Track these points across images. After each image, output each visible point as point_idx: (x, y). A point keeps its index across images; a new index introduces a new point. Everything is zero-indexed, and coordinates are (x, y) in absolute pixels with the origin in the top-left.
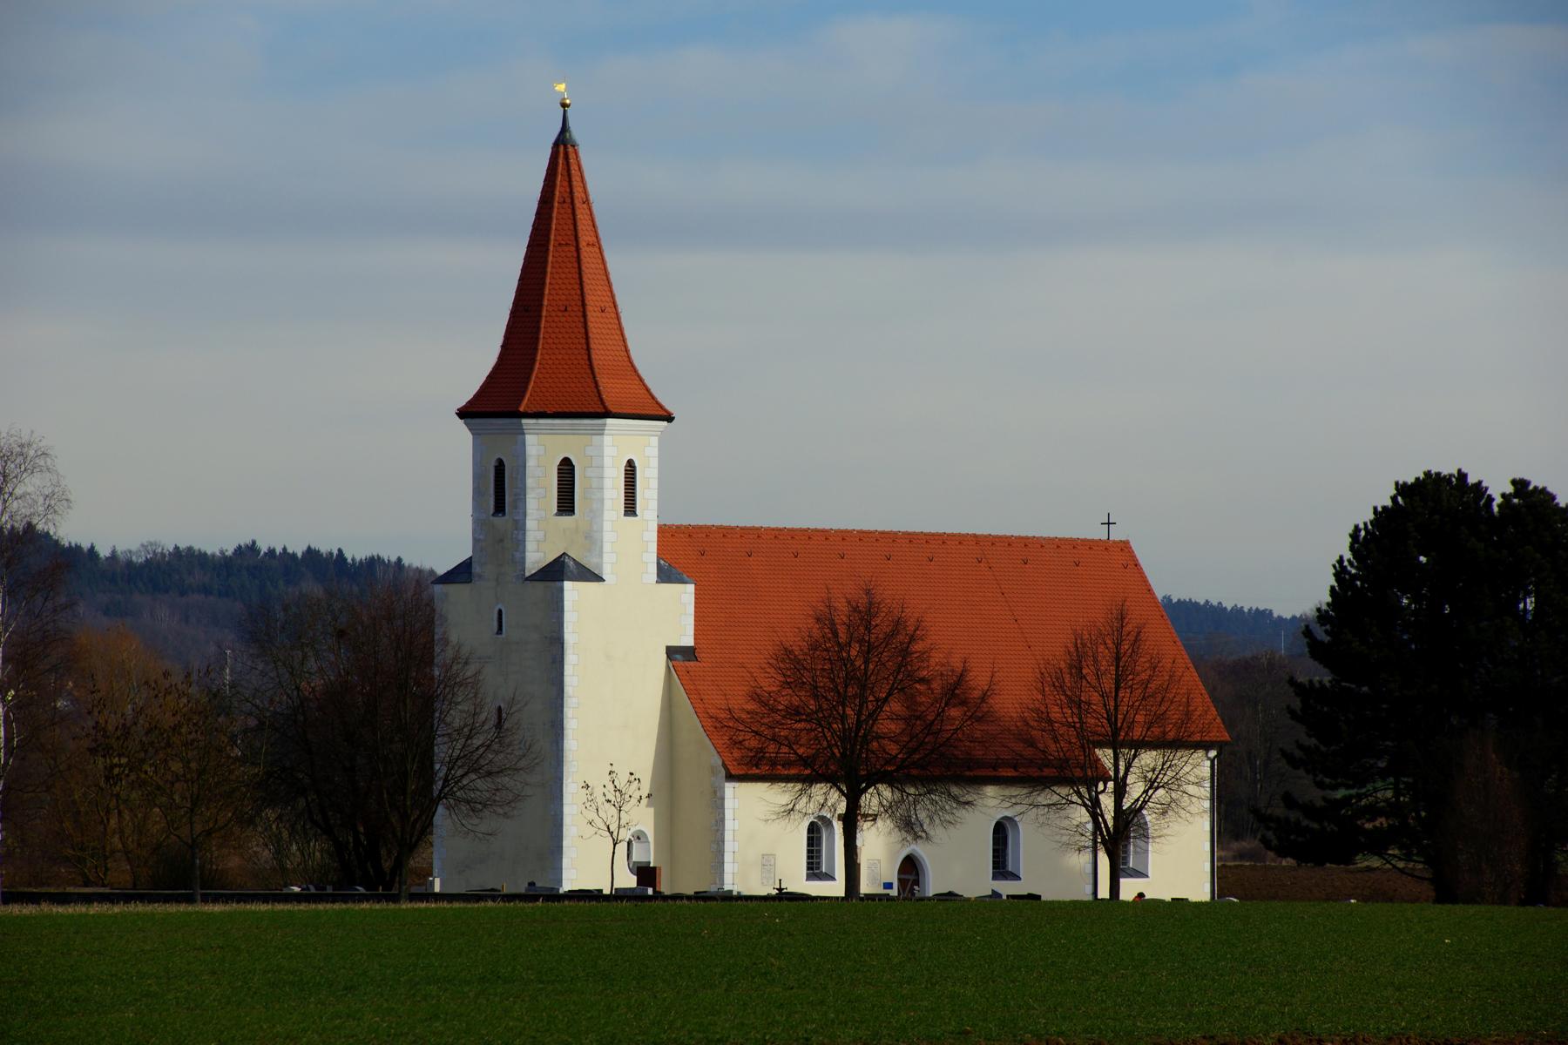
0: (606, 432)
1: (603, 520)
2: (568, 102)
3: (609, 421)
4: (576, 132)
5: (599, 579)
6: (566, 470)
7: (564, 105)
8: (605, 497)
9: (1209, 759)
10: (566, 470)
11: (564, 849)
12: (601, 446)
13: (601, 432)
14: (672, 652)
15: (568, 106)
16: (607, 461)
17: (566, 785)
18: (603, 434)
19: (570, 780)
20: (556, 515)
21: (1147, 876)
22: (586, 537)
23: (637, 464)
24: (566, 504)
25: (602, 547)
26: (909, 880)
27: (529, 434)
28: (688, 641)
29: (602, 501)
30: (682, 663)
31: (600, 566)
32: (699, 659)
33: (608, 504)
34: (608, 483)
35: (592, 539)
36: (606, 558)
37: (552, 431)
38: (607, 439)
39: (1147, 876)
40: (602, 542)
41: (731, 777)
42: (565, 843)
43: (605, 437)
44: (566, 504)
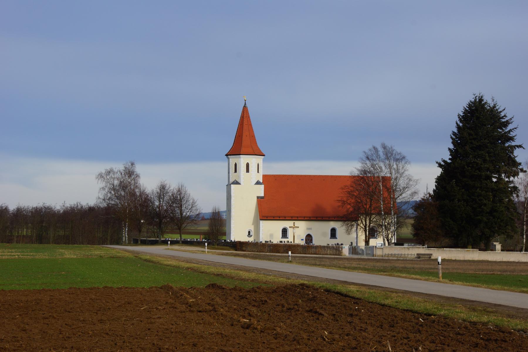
3: (241, 156)
4: (247, 105)
6: (236, 165)
7: (245, 100)
10: (236, 165)
13: (240, 158)
14: (258, 197)
16: (242, 163)
24: (236, 171)
28: (262, 195)
29: (241, 170)
31: (240, 182)
33: (242, 171)
34: (242, 167)
35: (239, 177)
37: (234, 158)
38: (242, 159)
41: (261, 220)
42: (231, 232)
44: (236, 171)
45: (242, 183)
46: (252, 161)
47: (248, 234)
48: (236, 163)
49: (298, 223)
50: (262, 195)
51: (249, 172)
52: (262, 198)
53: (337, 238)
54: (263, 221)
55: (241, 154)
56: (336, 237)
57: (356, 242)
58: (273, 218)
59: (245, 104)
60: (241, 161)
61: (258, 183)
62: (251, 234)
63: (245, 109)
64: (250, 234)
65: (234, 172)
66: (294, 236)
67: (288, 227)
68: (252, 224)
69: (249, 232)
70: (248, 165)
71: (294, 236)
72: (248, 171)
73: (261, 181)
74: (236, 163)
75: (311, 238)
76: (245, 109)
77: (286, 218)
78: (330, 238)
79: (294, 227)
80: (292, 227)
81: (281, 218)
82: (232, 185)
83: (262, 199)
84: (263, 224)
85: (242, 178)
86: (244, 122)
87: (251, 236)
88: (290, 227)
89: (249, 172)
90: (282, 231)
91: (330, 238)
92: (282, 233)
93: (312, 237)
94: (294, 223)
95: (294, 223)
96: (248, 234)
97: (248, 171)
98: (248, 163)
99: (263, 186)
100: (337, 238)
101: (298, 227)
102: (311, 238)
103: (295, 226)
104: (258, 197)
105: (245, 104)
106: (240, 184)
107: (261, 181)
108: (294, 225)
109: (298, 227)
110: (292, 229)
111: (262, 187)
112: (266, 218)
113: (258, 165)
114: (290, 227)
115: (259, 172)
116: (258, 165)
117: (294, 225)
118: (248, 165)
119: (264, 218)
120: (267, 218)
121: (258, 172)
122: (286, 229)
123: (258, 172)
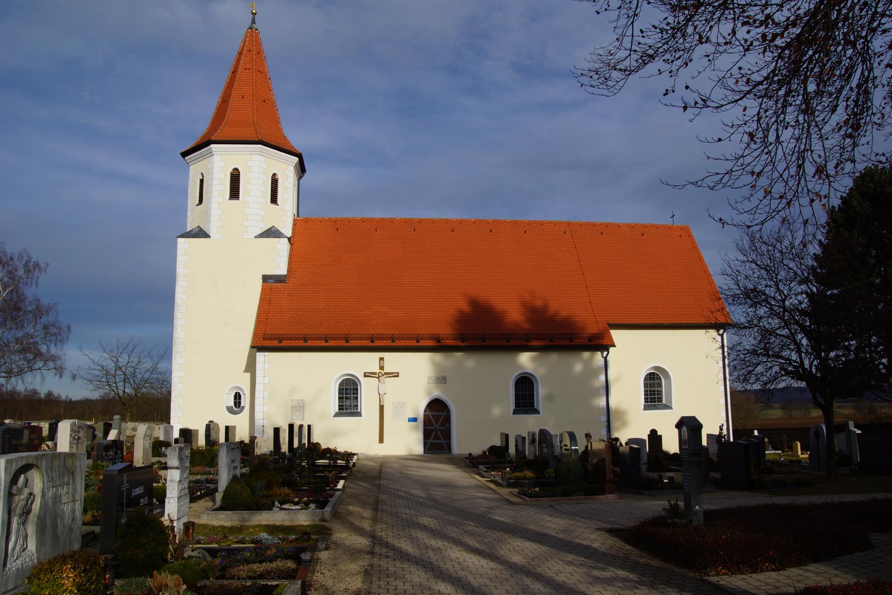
0: (214, 153)
2: (254, 12)
3: (212, 146)
5: (207, 236)
7: (253, 13)
9: (719, 334)
13: (211, 154)
14: (265, 278)
15: (255, 14)
16: (216, 170)
18: (213, 155)
20: (197, 205)
21: (672, 409)
26: (441, 416)
28: (282, 270)
29: (211, 192)
33: (215, 193)
34: (216, 182)
35: (207, 215)
37: (197, 160)
38: (216, 158)
39: (672, 409)
45: (212, 232)
47: (235, 403)
49: (394, 360)
50: (282, 270)
52: (278, 279)
53: (537, 412)
54: (267, 354)
55: (213, 138)
56: (535, 407)
57: (606, 424)
58: (301, 343)
59: (253, 21)
60: (215, 164)
61: (271, 233)
62: (242, 405)
64: (240, 403)
66: (382, 408)
67: (360, 376)
68: (244, 370)
69: (238, 397)
70: (235, 178)
71: (382, 408)
72: (235, 193)
75: (444, 414)
77: (353, 343)
78: (515, 412)
79: (381, 374)
80: (375, 373)
81: (331, 343)
82: (180, 240)
83: (278, 284)
84: (267, 365)
85: (214, 218)
86: (242, 62)
87: (243, 407)
88: (366, 375)
90: (341, 391)
91: (515, 412)
92: (339, 398)
93: (449, 411)
94: (382, 359)
95: (382, 359)
97: (235, 193)
98: (236, 169)
100: (537, 412)
101: (396, 375)
102: (444, 414)
103: (386, 370)
104: (265, 278)
105: (253, 21)
106: (209, 237)
108: (382, 368)
109: (396, 375)
110: (374, 381)
111: (282, 247)
112: (275, 343)
113: (275, 182)
114: (366, 375)
115: (279, 201)
116: (275, 182)
117: (382, 368)
118: (235, 178)
119: (267, 343)
120: (280, 341)
121: (274, 200)
122: (355, 384)
123: (274, 200)
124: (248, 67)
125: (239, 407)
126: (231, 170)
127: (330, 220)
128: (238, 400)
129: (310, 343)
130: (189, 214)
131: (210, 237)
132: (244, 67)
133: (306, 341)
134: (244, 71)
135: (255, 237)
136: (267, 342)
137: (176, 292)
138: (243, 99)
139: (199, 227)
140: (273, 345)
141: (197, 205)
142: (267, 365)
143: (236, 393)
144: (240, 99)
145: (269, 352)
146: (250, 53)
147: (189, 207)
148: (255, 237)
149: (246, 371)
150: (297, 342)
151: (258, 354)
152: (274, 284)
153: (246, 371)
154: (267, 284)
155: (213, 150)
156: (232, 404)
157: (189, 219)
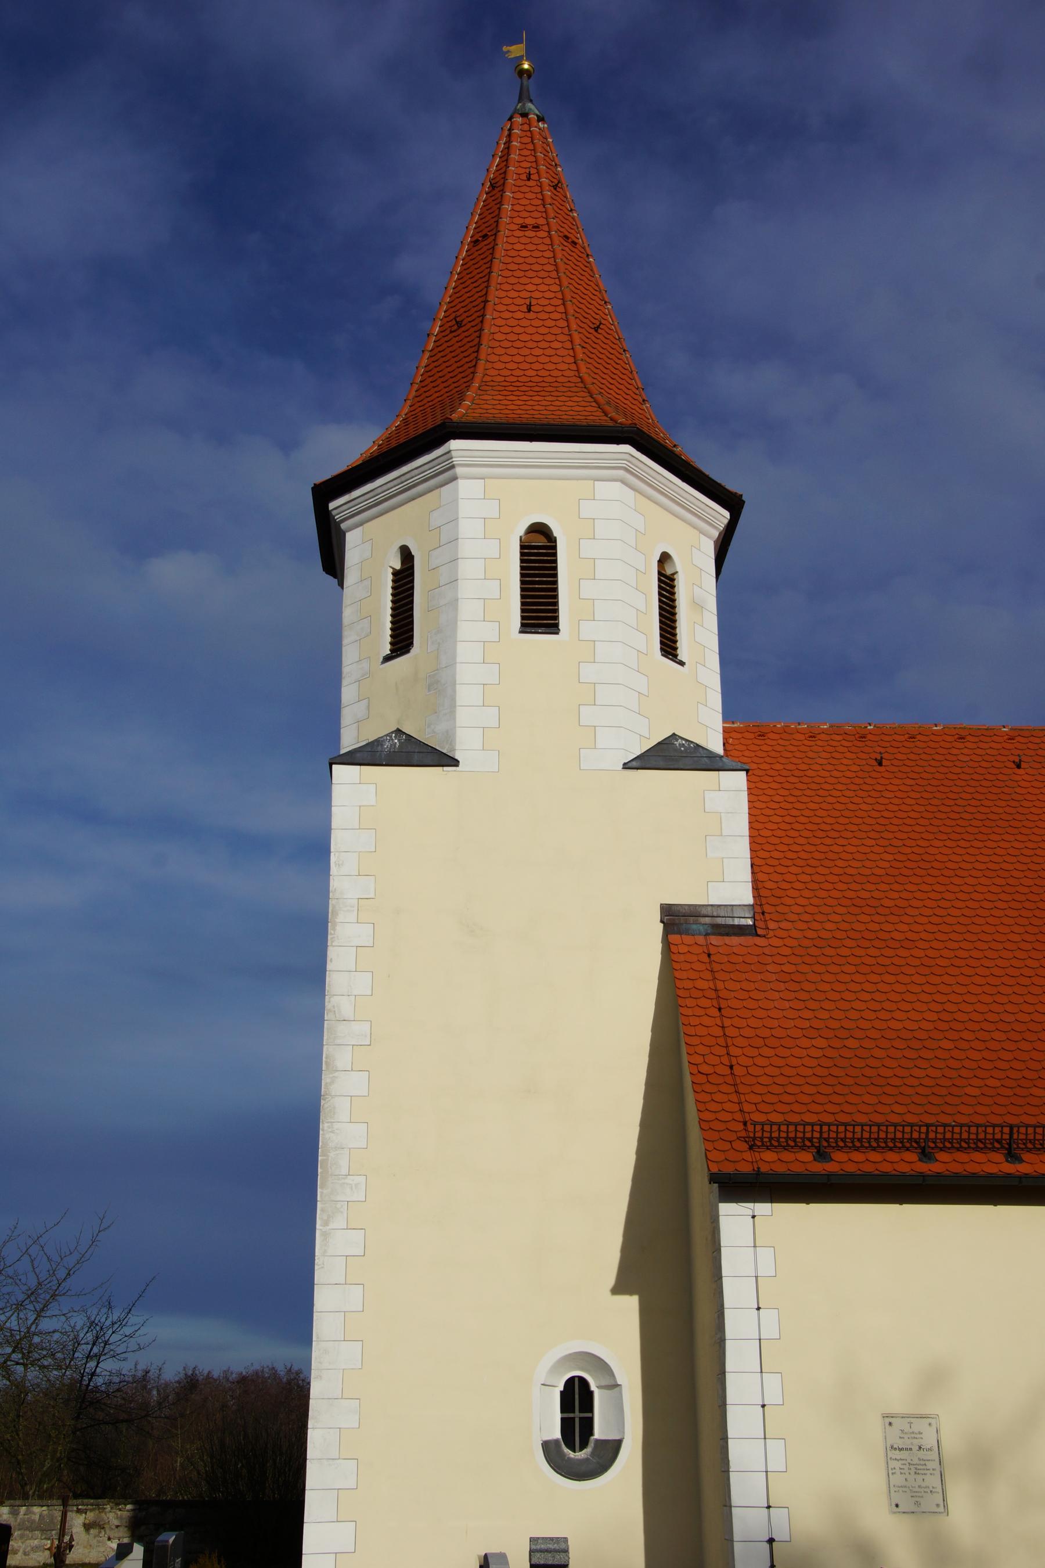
0: (459, 471)
1: (455, 642)
3: (455, 444)
8: (459, 596)
11: (313, 1403)
12: (455, 501)
13: (447, 472)
16: (468, 528)
17: (326, 1235)
18: (455, 478)
19: (339, 1222)
20: (387, 659)
22: (429, 687)
23: (557, 532)
25: (453, 699)
27: (350, 529)
29: (454, 603)
30: (701, 940)
31: (450, 736)
32: (760, 931)
33: (468, 609)
34: (469, 570)
36: (463, 716)
37: (379, 504)
40: (454, 684)
43: (460, 481)
46: (588, 509)
47: (567, 1425)
48: (406, 555)
51: (552, 627)
54: (762, 1208)
60: (465, 508)
62: (598, 1433)
63: (633, 765)
65: (387, 650)
68: (610, 1278)
73: (715, 744)
74: (406, 555)
76: (633, 765)
84: (765, 1255)
85: (466, 695)
86: (506, 207)
87: (611, 1450)
89: (552, 627)
96: (556, 1433)
98: (540, 530)
99: (736, 781)
106: (454, 762)
107: (715, 744)
113: (667, 585)
115: (682, 655)
116: (667, 585)
119: (770, 1161)
120: (821, 1155)
121: (669, 647)
123: (669, 647)
124: (530, 221)
125: (584, 1445)
126: (521, 530)
127: (836, 730)
128: (577, 1414)
129: (945, 1163)
130: (348, 693)
131: (454, 762)
132: (520, 221)
133: (925, 1155)
134: (518, 233)
135: (626, 766)
136: (769, 1156)
137: (329, 967)
138: (531, 315)
139: (399, 732)
140: (797, 1168)
141: (387, 659)
142: (765, 1255)
143: (570, 1382)
144: (519, 315)
145: (772, 1200)
146: (531, 183)
147: (346, 670)
148: (626, 766)
149: (619, 1289)
150: (891, 1156)
151: (726, 1209)
152: (714, 940)
153: (619, 1289)
154: (688, 940)
155: (456, 460)
156: (557, 1434)
157: (349, 715)
